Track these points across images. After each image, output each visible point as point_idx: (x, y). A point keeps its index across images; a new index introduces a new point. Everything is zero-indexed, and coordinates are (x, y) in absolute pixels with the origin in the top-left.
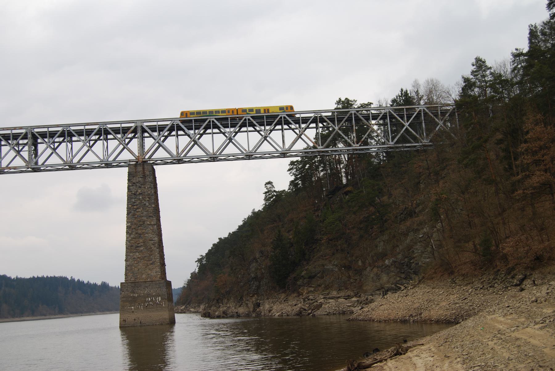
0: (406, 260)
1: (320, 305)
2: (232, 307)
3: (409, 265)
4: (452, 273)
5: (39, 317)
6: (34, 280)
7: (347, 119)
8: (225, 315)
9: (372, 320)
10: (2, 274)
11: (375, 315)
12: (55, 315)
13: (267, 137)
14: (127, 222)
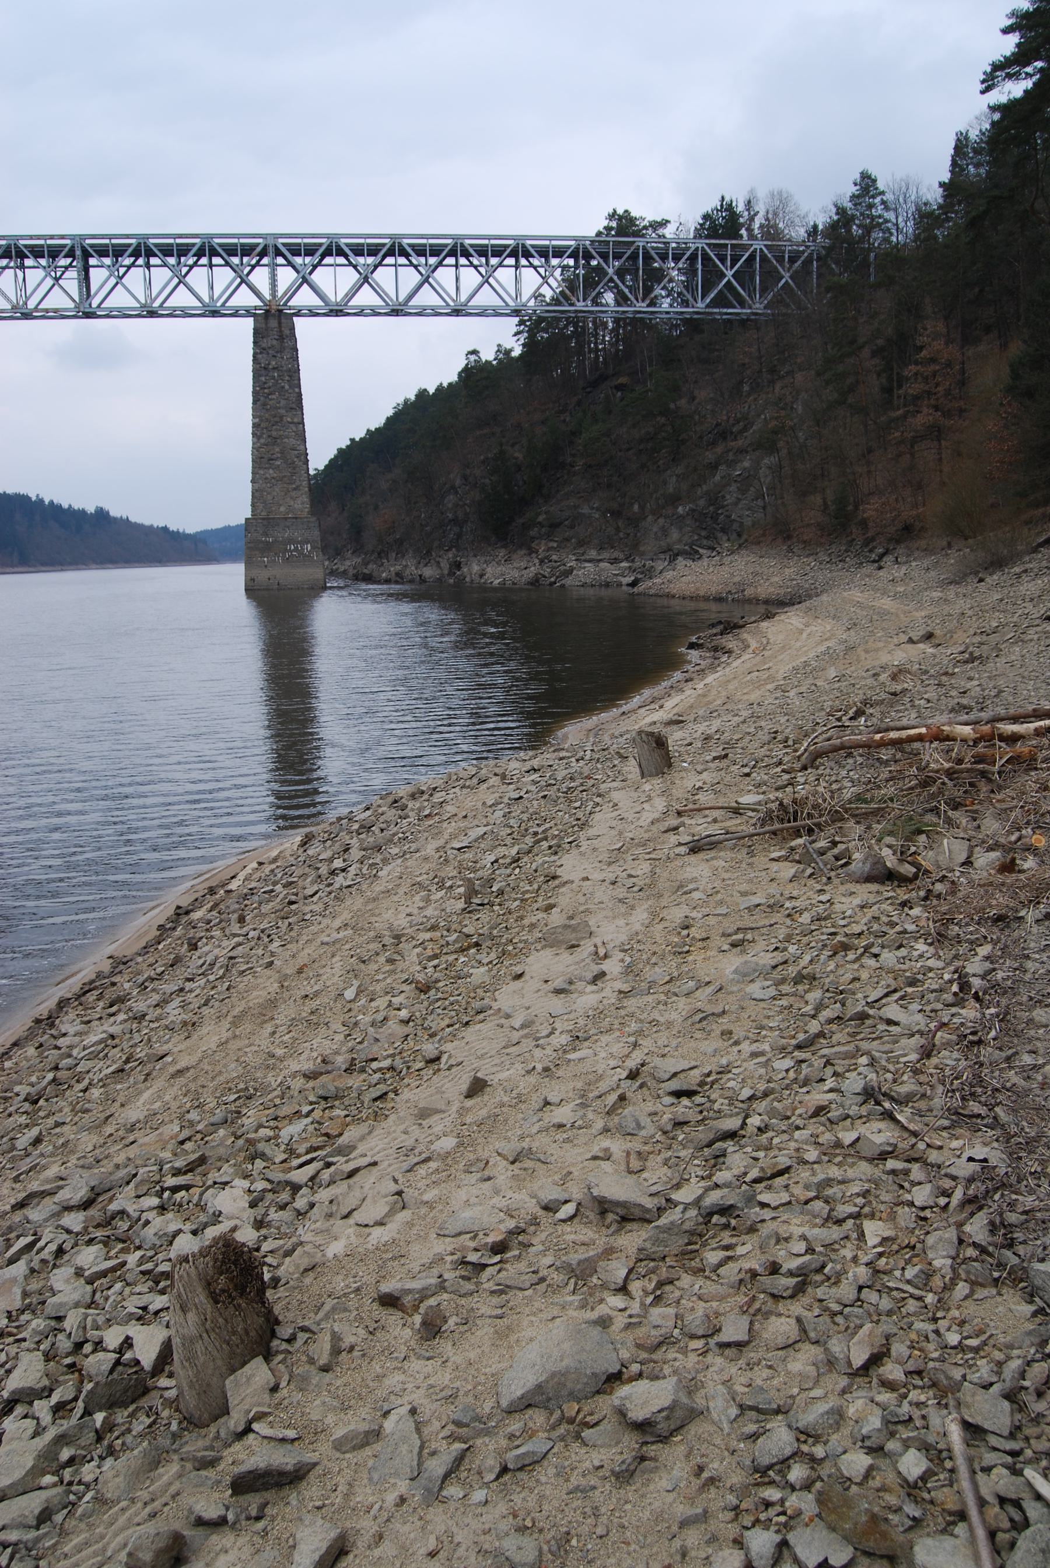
0: (711, 508)
1: (571, 571)
2: (410, 566)
3: (714, 518)
4: (789, 537)
7: (623, 250)
8: (399, 578)
9: (670, 596)
10: (11, 488)
11: (675, 588)
12: (12, 566)
14: (254, 417)
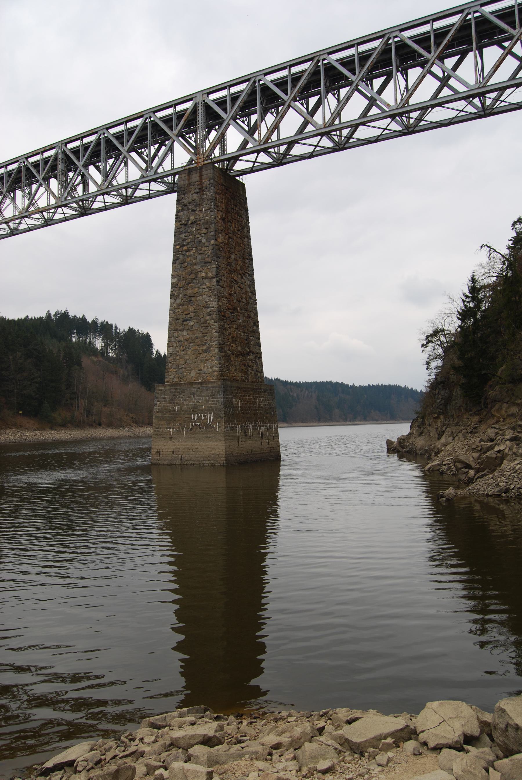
1: (501, 457)
5: (371, 422)
6: (370, 388)
12: (386, 420)
13: (449, 77)
14: (173, 277)
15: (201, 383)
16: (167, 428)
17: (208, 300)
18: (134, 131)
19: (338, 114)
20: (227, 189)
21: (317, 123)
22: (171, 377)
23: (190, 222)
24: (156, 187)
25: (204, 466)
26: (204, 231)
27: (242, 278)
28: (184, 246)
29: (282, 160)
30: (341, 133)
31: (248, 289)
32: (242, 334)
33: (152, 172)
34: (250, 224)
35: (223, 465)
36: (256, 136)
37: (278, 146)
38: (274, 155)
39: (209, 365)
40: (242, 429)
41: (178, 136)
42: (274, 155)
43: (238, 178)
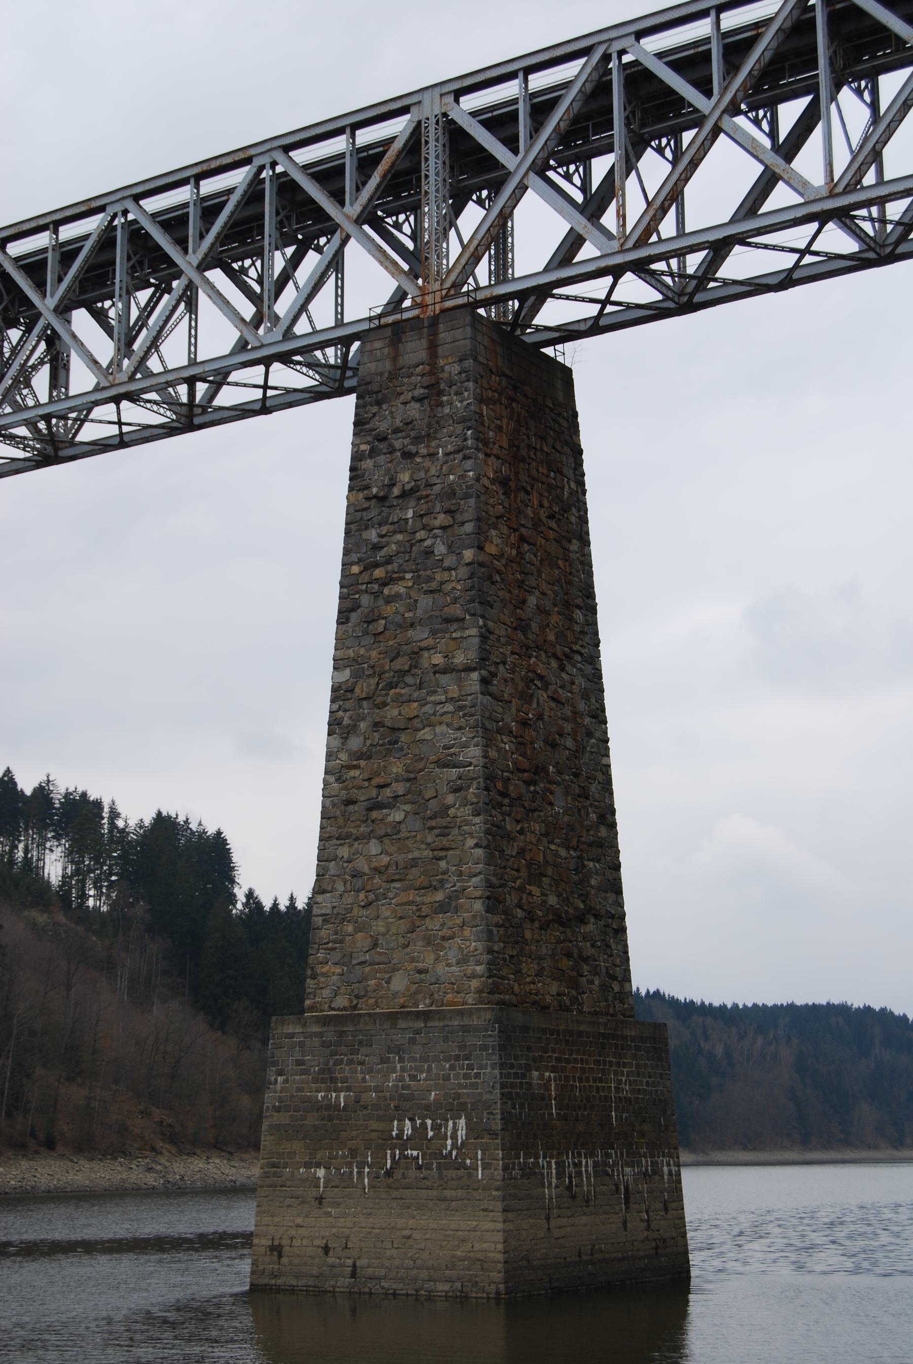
15: (426, 1016)
16: (307, 1165)
17: (452, 739)
18: (221, 206)
19: (871, 153)
20: (515, 388)
21: (805, 183)
22: (326, 993)
23: (396, 491)
24: (285, 377)
25: (430, 1299)
26: (442, 519)
27: (562, 668)
28: (376, 565)
29: (692, 295)
30: (883, 212)
31: (582, 706)
32: (563, 852)
33: (277, 334)
34: (589, 497)
35: (498, 1299)
36: (609, 219)
37: (681, 254)
38: (668, 280)
39: (453, 955)
40: (560, 1175)
41: (359, 221)
42: (668, 280)
43: (549, 351)
